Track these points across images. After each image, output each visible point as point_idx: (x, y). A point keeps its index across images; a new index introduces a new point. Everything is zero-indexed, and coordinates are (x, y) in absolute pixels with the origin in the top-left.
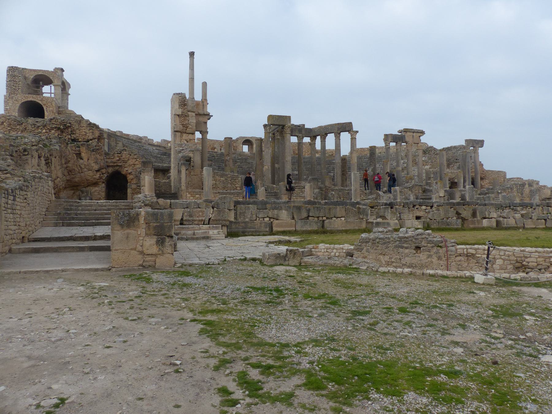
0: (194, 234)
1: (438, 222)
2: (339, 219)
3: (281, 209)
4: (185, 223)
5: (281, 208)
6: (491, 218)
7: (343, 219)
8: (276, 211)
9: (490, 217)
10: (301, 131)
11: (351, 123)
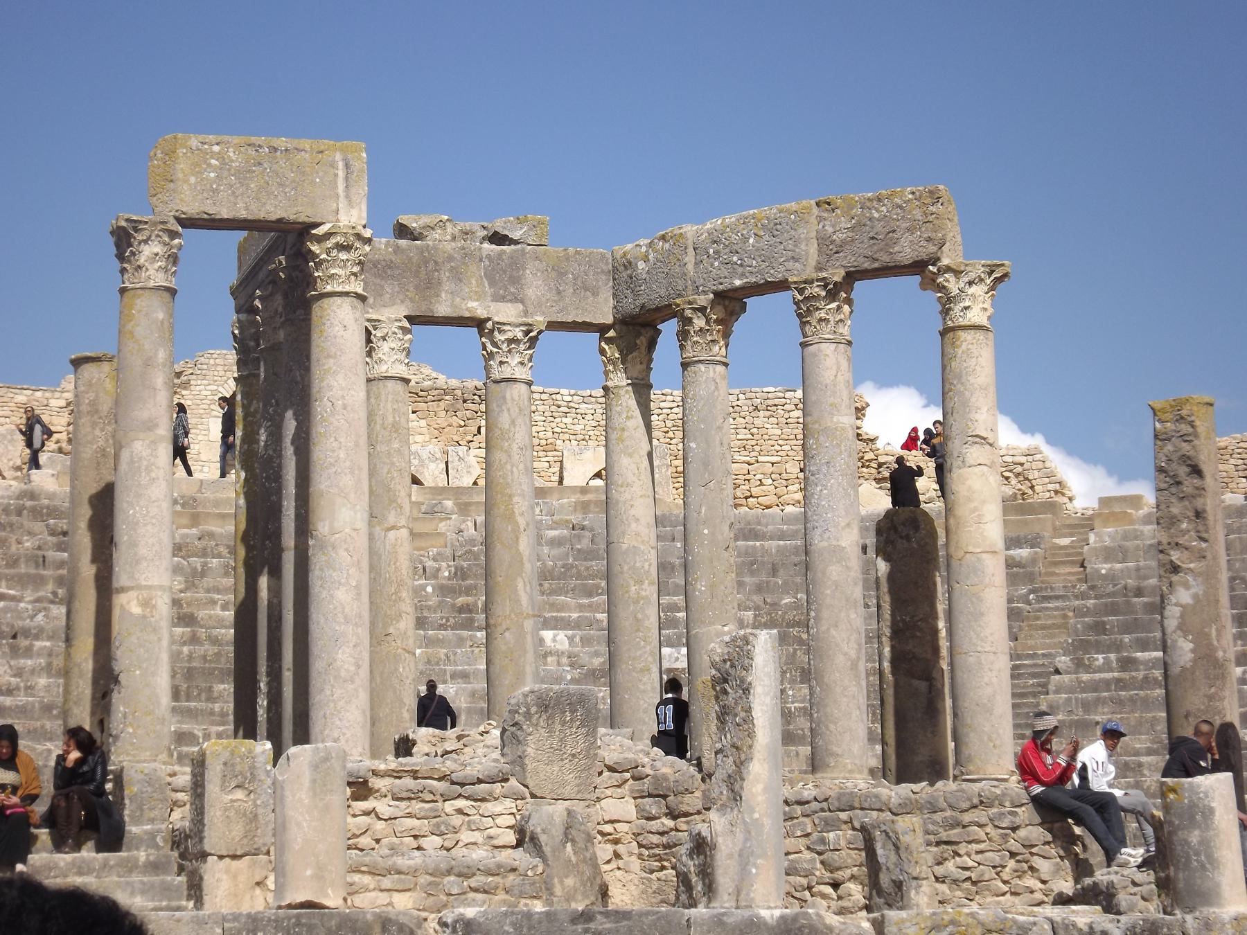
10: (516, 281)
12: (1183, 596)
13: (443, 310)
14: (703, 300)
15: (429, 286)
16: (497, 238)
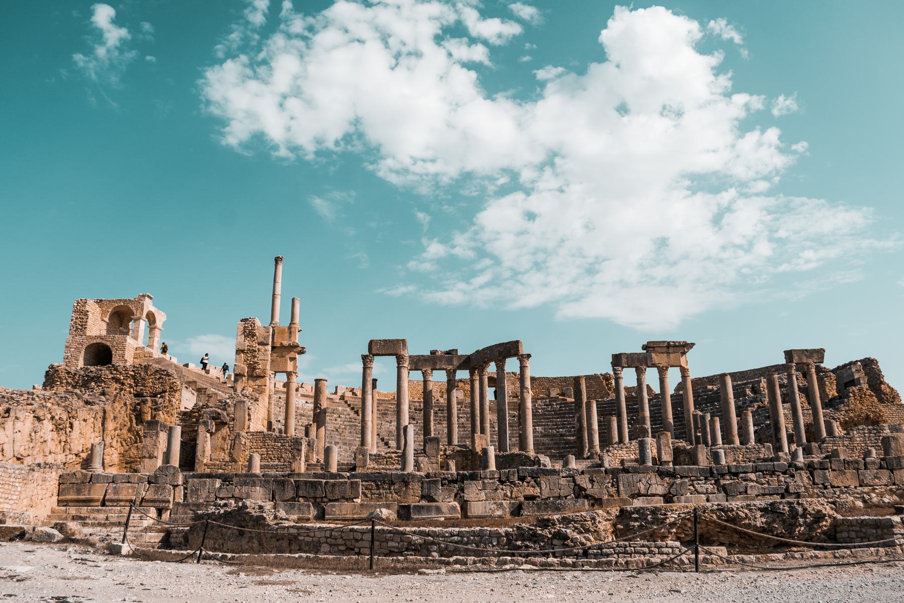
0: (107, 519)
3: (254, 485)
4: (107, 503)
5: (254, 482)
6: (653, 495)
8: (245, 489)
9: (649, 492)
11: (517, 342)
15: (435, 363)
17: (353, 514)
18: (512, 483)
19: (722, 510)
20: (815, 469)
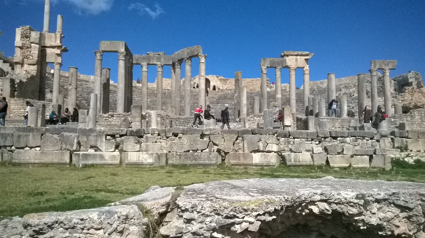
1: (180, 156)
2: (33, 149)
6: (270, 152)
7: (38, 149)
9: (267, 149)
10: (160, 59)
12: (236, 95)
13: (151, 63)
14: (177, 61)
15: (150, 60)
16: (159, 55)
17: (35, 160)
18: (168, 138)
19: (325, 201)
20: (395, 137)
